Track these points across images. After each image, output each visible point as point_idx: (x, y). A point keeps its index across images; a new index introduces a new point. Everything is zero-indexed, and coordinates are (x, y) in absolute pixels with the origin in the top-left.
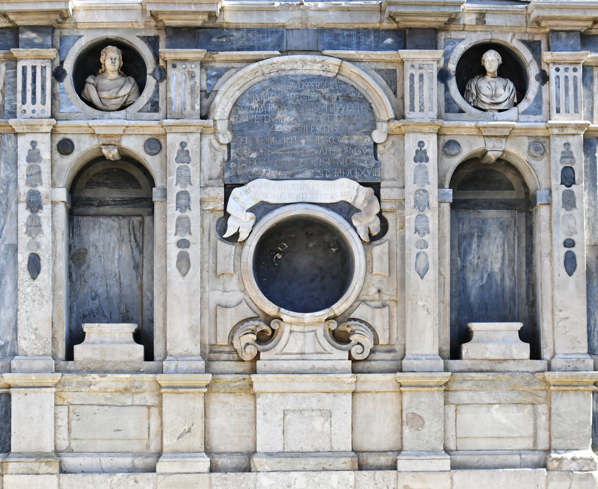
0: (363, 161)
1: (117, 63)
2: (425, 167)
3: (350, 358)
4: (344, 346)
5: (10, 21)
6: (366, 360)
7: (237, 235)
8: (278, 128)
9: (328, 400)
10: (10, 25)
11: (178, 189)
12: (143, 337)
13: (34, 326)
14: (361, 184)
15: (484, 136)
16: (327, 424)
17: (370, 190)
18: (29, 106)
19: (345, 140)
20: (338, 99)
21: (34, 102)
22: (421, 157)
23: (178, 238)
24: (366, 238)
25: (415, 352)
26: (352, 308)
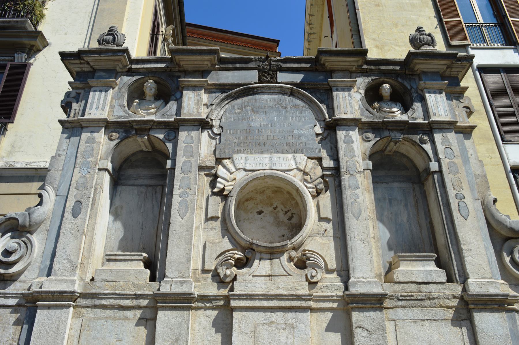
0: (309, 144)
1: (153, 90)
2: (352, 146)
3: (307, 280)
5: (91, 67)
7: (223, 190)
8: (252, 124)
10: (91, 70)
11: (184, 159)
12: (149, 264)
13: (68, 253)
14: (309, 158)
15: (389, 130)
16: (290, 336)
19: (297, 132)
20: (291, 108)
23: (182, 190)
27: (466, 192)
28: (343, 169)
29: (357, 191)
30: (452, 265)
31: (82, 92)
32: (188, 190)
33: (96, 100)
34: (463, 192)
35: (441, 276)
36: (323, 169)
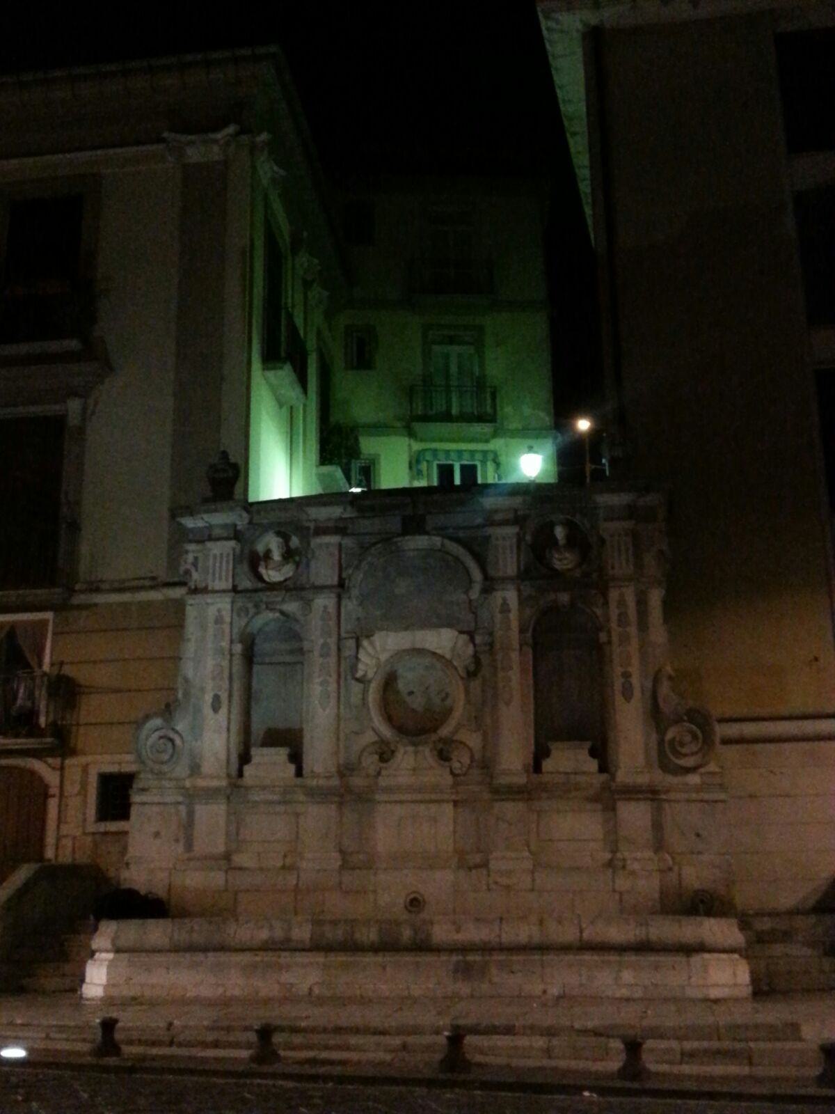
4: (447, 764)
5: (206, 522)
6: (465, 775)
9: (434, 808)
10: (207, 525)
11: (322, 641)
17: (465, 637)
18: (217, 582)
21: (220, 578)
22: (505, 609)
23: (321, 679)
24: (464, 674)
25: (504, 767)
26: (456, 731)
27: (635, 669)
28: (498, 646)
29: (510, 673)
30: (602, 753)
31: (199, 555)
32: (328, 678)
33: (217, 569)
34: (630, 669)
35: (593, 765)
36: (475, 645)
